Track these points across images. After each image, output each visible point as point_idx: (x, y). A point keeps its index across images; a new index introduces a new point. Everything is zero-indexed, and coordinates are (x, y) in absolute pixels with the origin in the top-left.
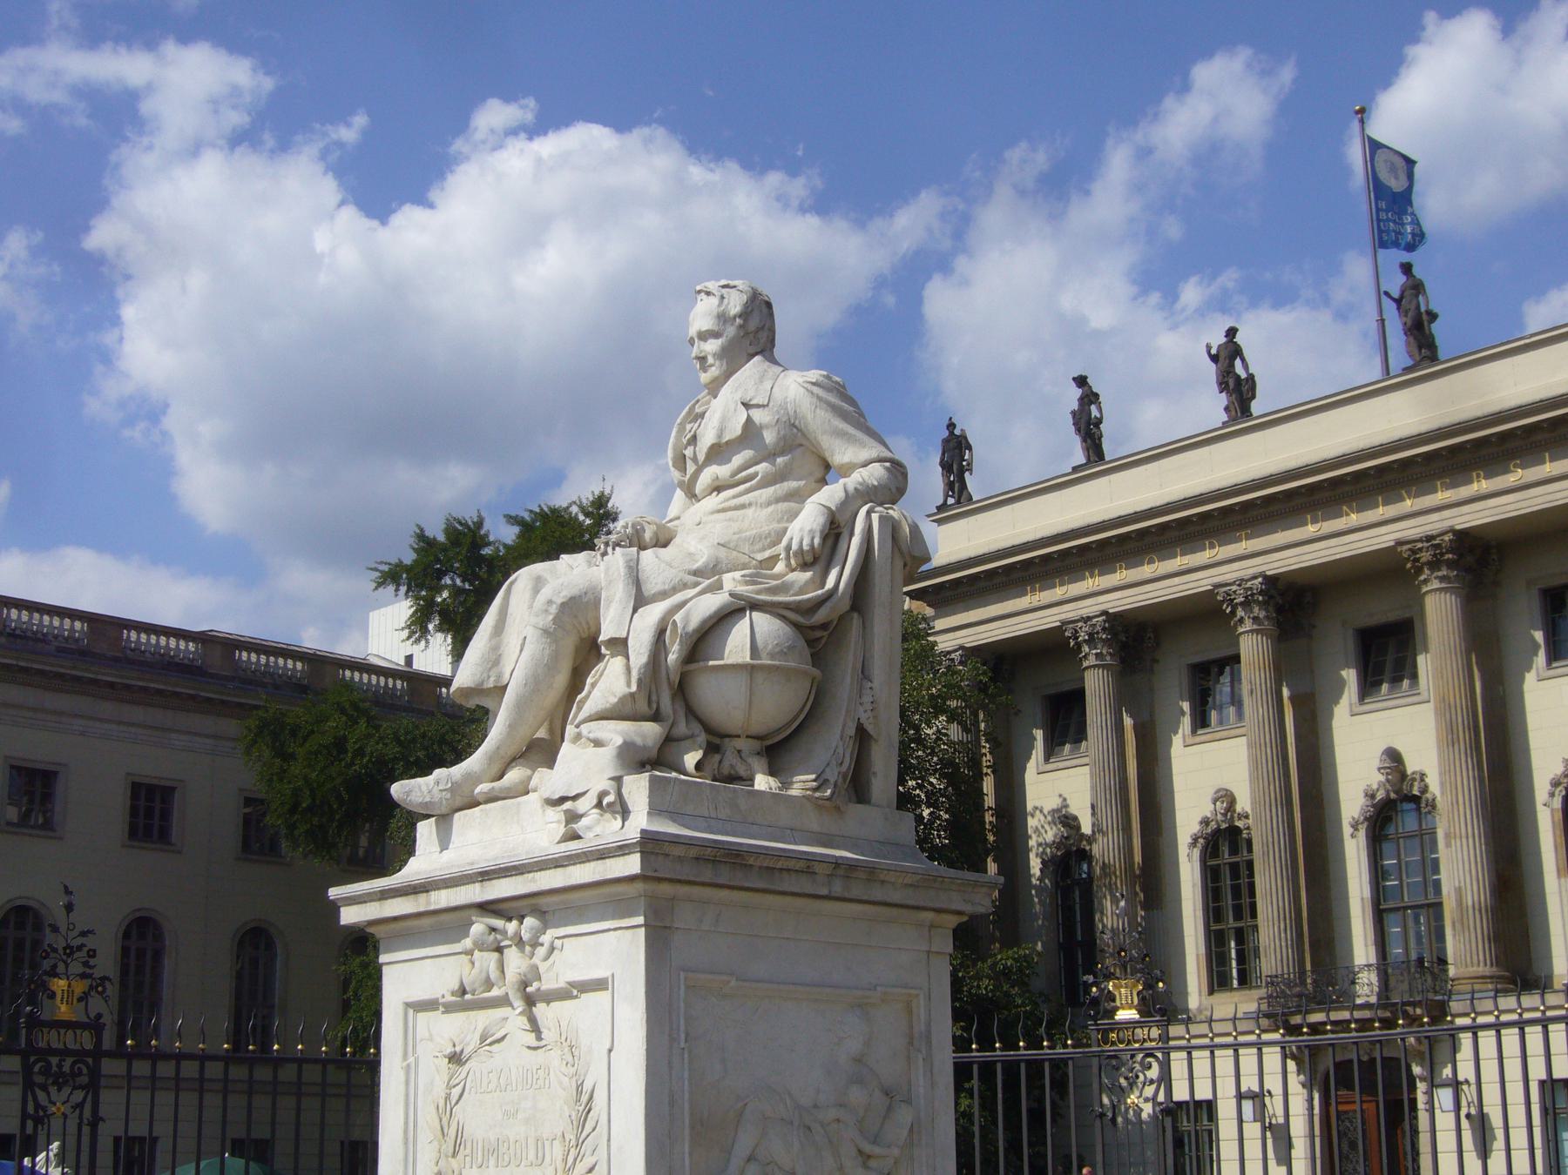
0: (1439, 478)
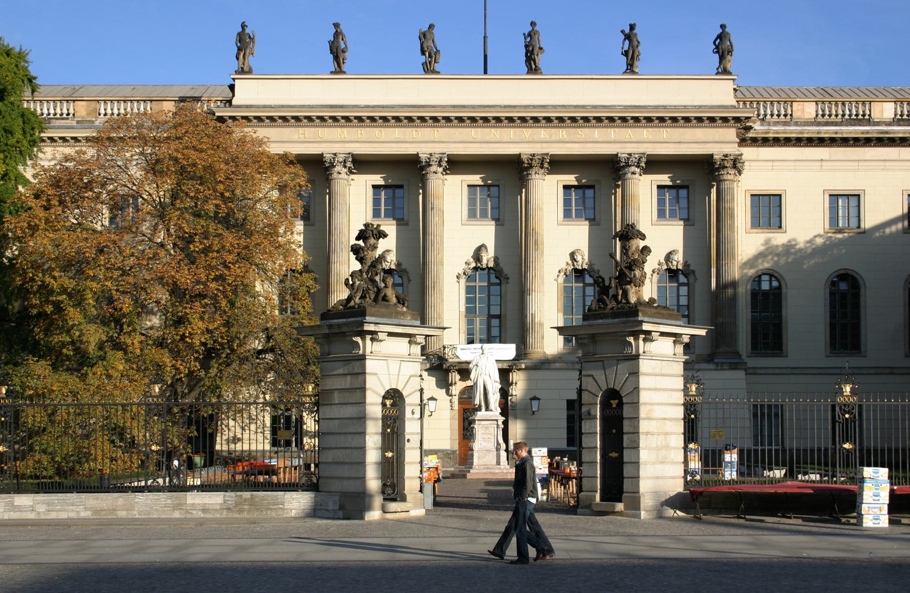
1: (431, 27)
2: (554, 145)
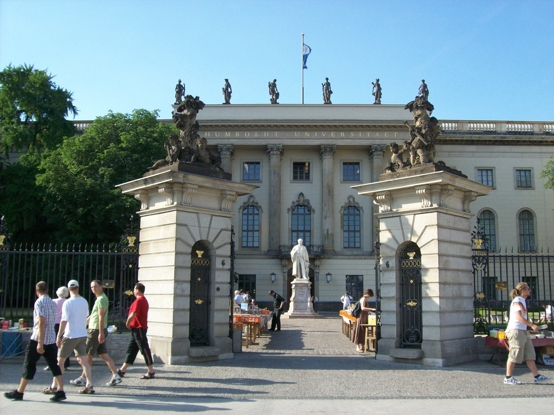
1: (275, 81)
2: (338, 140)
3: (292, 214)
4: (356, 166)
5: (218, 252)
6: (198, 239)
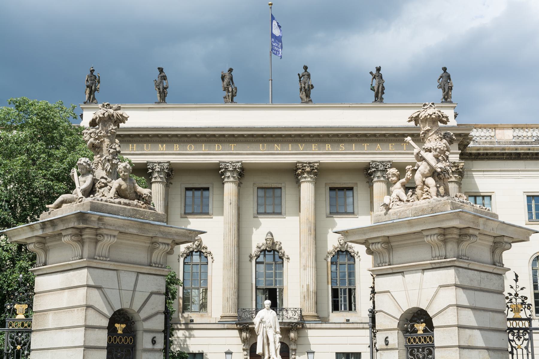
0: (314, 143)
1: (231, 70)
3: (257, 263)
4: (349, 193)
5: (147, 325)
6: (117, 307)
